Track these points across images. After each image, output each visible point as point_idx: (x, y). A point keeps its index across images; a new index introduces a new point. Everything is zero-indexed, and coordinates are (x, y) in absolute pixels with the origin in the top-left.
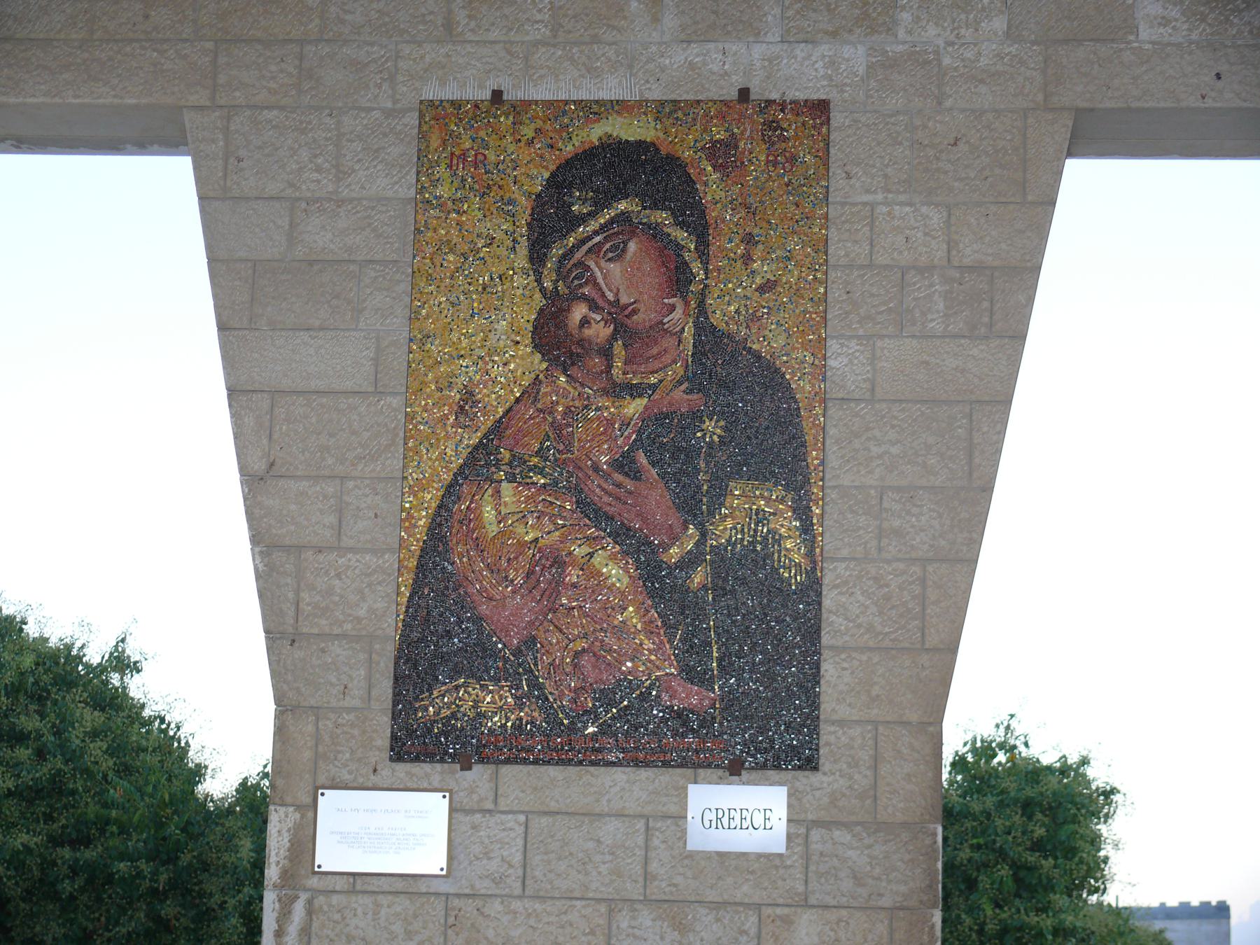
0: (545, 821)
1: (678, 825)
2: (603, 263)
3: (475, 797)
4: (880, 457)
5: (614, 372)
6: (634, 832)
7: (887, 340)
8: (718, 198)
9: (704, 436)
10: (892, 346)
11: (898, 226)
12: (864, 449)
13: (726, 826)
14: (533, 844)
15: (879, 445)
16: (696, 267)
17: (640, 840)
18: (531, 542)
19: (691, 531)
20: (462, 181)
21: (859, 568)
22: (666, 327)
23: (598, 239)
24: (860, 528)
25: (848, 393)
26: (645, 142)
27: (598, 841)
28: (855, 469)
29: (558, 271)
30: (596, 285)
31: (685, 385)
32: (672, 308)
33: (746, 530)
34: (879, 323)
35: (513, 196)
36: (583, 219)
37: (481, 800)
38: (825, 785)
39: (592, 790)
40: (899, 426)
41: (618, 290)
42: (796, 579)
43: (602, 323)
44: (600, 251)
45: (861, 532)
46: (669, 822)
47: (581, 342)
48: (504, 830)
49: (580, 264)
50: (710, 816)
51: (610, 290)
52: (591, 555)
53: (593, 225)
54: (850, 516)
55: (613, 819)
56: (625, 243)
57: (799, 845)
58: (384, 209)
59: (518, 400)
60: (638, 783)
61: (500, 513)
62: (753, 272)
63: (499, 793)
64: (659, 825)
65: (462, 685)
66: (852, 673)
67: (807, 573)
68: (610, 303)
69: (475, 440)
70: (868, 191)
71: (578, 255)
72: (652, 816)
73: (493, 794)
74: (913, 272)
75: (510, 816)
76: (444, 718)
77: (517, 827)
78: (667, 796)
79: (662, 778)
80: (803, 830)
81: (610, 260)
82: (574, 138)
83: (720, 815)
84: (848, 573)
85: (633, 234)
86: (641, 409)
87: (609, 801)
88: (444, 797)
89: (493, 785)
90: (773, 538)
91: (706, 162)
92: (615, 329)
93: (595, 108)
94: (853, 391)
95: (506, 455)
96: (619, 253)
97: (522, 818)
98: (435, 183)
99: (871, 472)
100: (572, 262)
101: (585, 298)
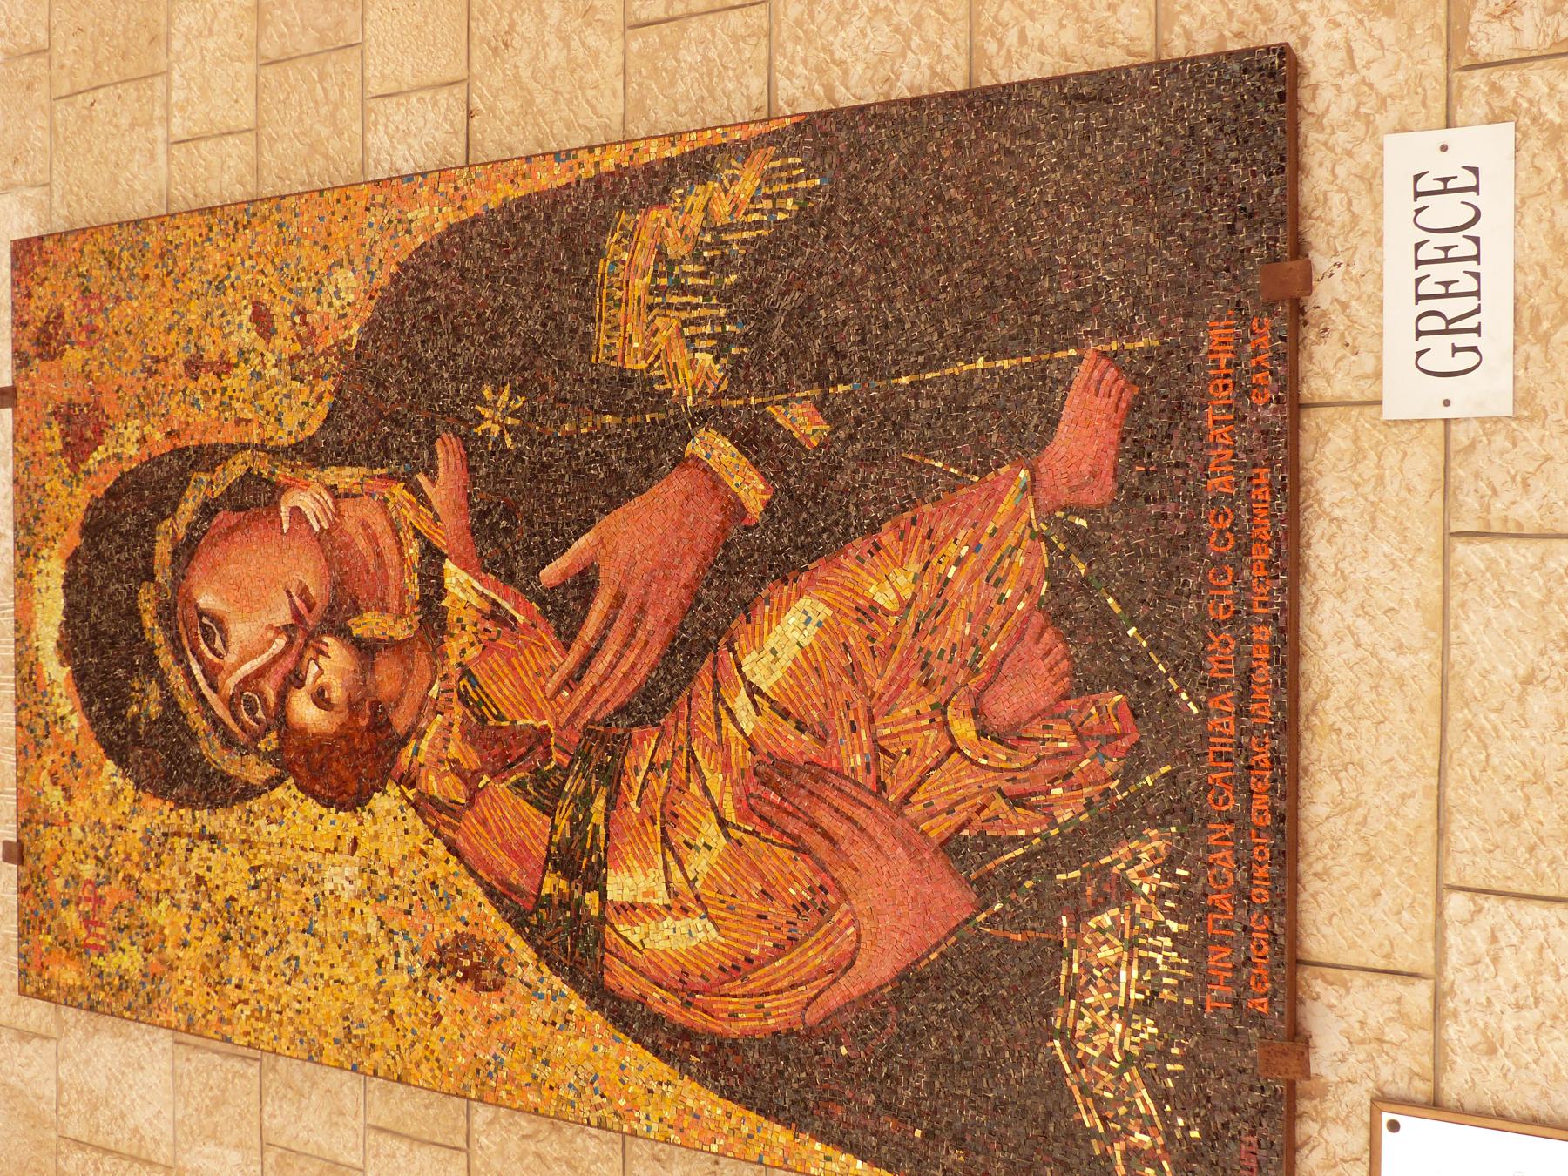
0: (1463, 836)
1: (1473, 446)
2: (231, 658)
3: (1394, 1033)
4: (565, 40)
5: (400, 632)
6: (1496, 576)
7: (368, 74)
8: (137, 434)
9: (509, 429)
10: (379, 60)
11: (200, 89)
12: (553, 78)
13: (1469, 304)
14: (1541, 877)
15: (546, 45)
16: (236, 469)
17: (1522, 554)
18: (727, 836)
19: (698, 450)
20: (121, 930)
21: (789, 47)
22: (326, 527)
23: (196, 669)
24: (706, 59)
25: (456, 133)
26: (66, 577)
27: (1528, 680)
28: (590, 93)
29: (244, 750)
30: (260, 673)
31: (421, 478)
32: (296, 511)
33: (695, 314)
34: (342, 93)
35: (139, 835)
36: (170, 702)
37: (1402, 1017)
38: (1337, 35)
39: (1368, 697)
40: (510, 14)
41: (271, 627)
42: (799, 178)
43: (322, 659)
44: (214, 666)
45: (713, 54)
46: (1460, 472)
47: (353, 706)
48: (1495, 960)
49: (231, 703)
50: (1440, 353)
51: (271, 642)
52: (753, 691)
53: (177, 679)
54: (681, 88)
55: (1453, 635)
56: (201, 614)
57: (1525, 82)
58: (186, 1081)
59: (452, 848)
60: (1345, 566)
61: (668, 908)
62: (241, 352)
63: (1381, 964)
64: (1472, 502)
65: (1069, 1047)
66: (1032, 15)
67: (785, 155)
68: (290, 643)
69: (527, 954)
70: (152, 157)
71: (221, 711)
72: (1446, 526)
73: (1385, 980)
74: (264, 44)
75: (1452, 937)
76: (1160, 1109)
77: (1486, 921)
78: (1380, 480)
79: (1328, 499)
80: (1478, 78)
81: (225, 645)
82: (61, 712)
83: (1436, 323)
84: (800, 70)
85: (191, 602)
86: (464, 576)
87: (1400, 648)
88: (1394, 1126)
89: (1358, 980)
90: (709, 246)
91: (91, 461)
92: (330, 634)
93: (25, 671)
94: (452, 125)
95: (553, 884)
96: (214, 626)
97: (1457, 904)
98: (125, 984)
99: (595, 55)
100: (230, 722)
101: (282, 697)
